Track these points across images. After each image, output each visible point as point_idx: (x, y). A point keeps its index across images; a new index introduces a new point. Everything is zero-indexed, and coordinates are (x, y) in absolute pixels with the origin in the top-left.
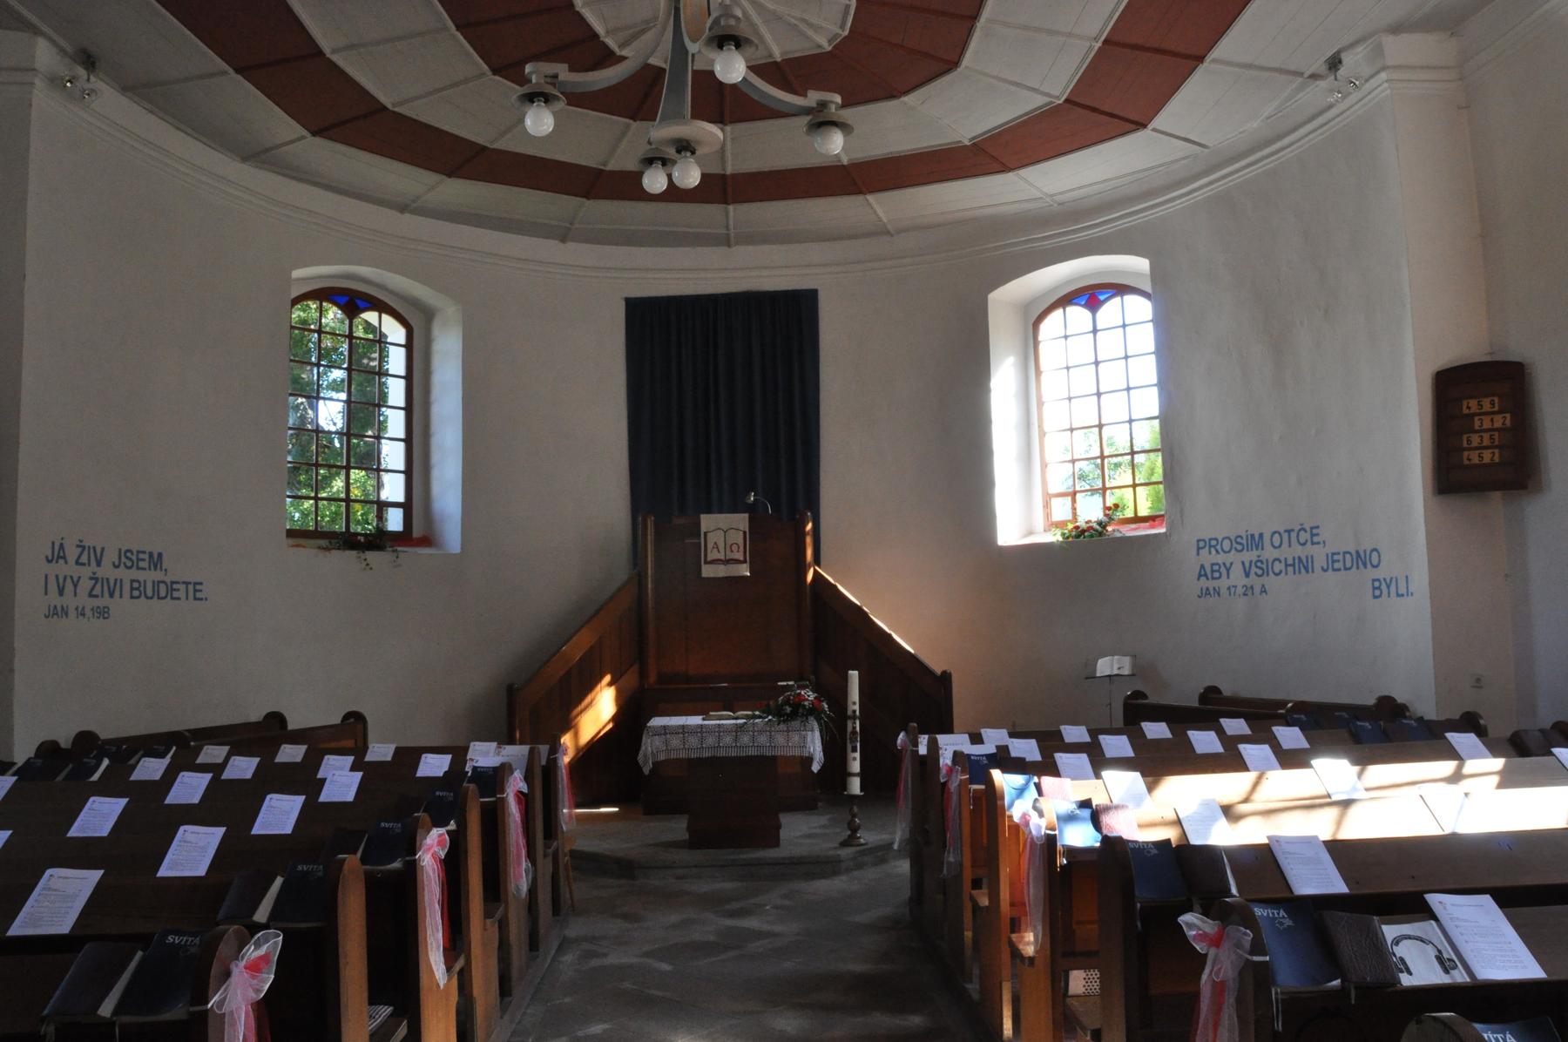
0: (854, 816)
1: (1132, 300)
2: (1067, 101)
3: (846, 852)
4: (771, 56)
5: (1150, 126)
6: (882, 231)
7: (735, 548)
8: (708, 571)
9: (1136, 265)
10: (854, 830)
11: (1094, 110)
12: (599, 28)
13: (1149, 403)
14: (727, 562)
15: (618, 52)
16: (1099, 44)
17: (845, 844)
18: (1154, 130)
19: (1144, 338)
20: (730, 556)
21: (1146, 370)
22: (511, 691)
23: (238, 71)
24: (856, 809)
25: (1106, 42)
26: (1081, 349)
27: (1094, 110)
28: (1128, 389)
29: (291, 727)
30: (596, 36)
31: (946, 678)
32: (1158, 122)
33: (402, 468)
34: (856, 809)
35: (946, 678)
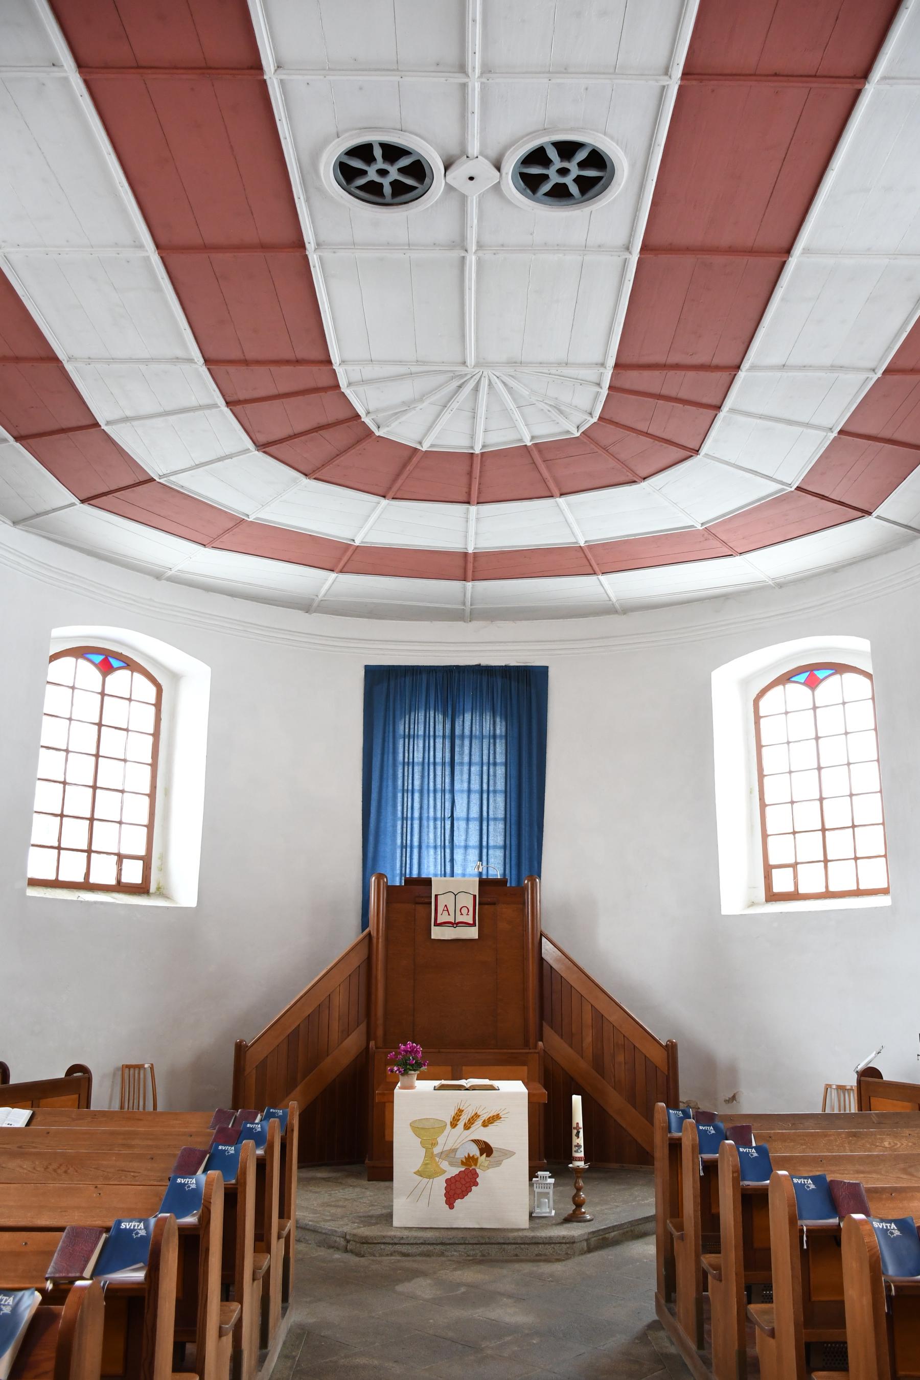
0: (579, 1189)
1: (848, 677)
2: (798, 488)
3: (575, 1231)
4: (521, 440)
5: (875, 514)
6: (608, 610)
7: (464, 911)
8: (437, 933)
9: (854, 647)
10: (579, 1205)
11: (823, 497)
12: (361, 411)
13: (868, 777)
14: (455, 924)
15: (377, 434)
16: (835, 434)
17: (568, 1220)
18: (878, 517)
19: (863, 715)
20: (460, 919)
21: (866, 746)
22: (240, 1048)
23: (17, 439)
24: (581, 1183)
25: (841, 432)
26: (802, 725)
27: (823, 497)
28: (849, 764)
29: (13, 1081)
30: (358, 416)
31: (671, 1049)
32: (878, 512)
33: (60, 878)
34: (581, 1183)
35: (671, 1049)
